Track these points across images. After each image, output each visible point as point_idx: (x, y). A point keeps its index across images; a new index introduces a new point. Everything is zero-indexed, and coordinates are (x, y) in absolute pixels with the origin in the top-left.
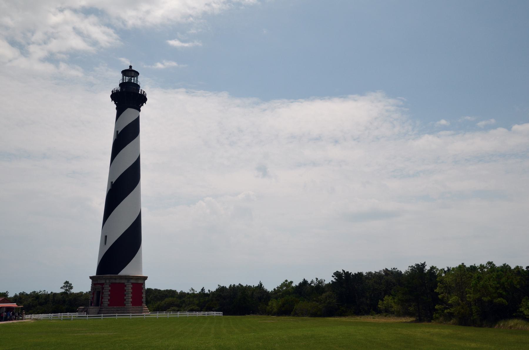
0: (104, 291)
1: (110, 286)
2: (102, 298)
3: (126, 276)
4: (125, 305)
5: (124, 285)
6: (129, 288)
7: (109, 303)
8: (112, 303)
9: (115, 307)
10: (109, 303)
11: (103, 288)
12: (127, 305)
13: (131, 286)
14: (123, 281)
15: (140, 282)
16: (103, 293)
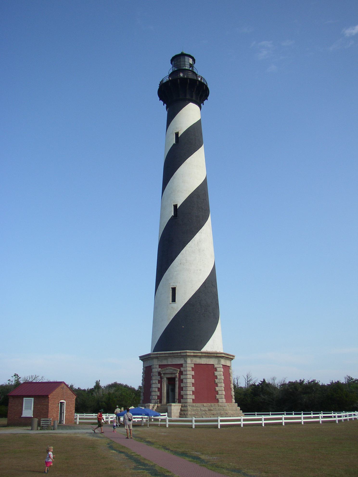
0: (182, 377)
1: (193, 369)
2: (181, 389)
3: (217, 353)
4: (217, 401)
5: (213, 368)
6: (220, 373)
7: (193, 397)
8: (199, 398)
9: (205, 404)
10: (193, 397)
11: (181, 373)
12: (220, 400)
13: (222, 370)
14: (211, 361)
15: (228, 363)
16: (181, 381)
